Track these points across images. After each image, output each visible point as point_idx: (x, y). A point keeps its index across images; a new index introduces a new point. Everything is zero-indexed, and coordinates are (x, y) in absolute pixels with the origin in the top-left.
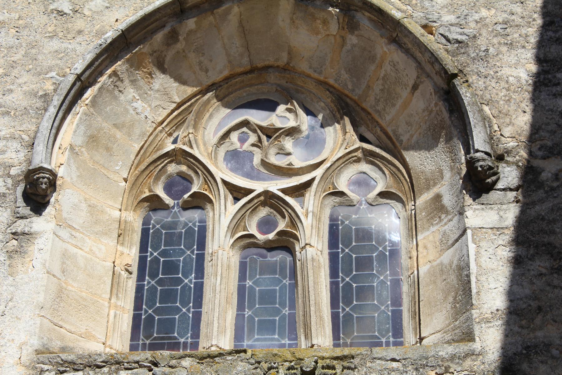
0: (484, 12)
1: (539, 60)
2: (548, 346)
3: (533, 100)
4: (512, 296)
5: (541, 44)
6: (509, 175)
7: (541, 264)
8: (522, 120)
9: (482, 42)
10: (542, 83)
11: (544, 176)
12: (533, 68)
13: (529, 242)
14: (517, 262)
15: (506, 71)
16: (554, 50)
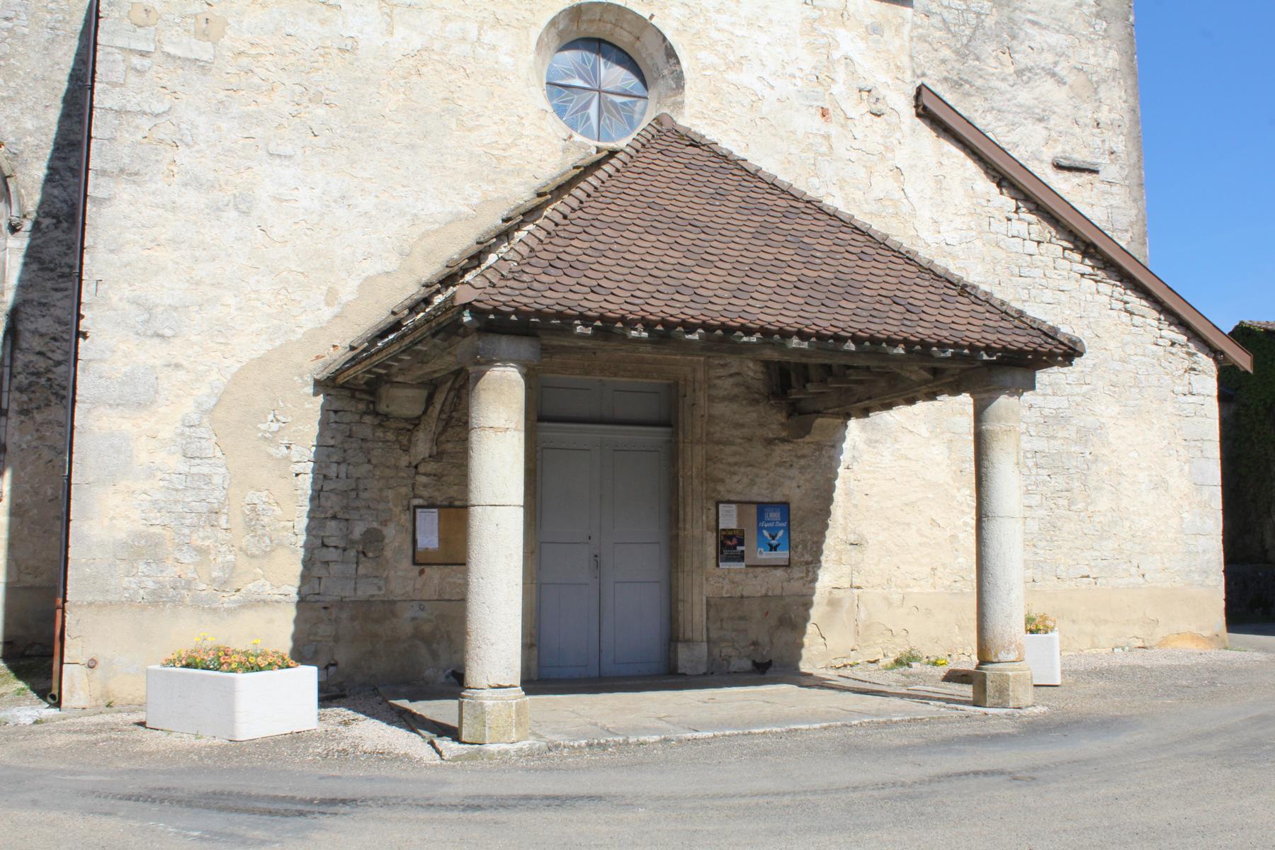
0: (29, 138)
1: (49, 168)
2: (32, 300)
3: (44, 189)
4: (20, 280)
5: (51, 160)
6: (27, 225)
7: (35, 266)
8: (37, 197)
9: (25, 155)
10: (49, 180)
11: (43, 226)
12: (45, 171)
13: (32, 256)
14: (25, 264)
15: (34, 172)
16: (58, 164)
